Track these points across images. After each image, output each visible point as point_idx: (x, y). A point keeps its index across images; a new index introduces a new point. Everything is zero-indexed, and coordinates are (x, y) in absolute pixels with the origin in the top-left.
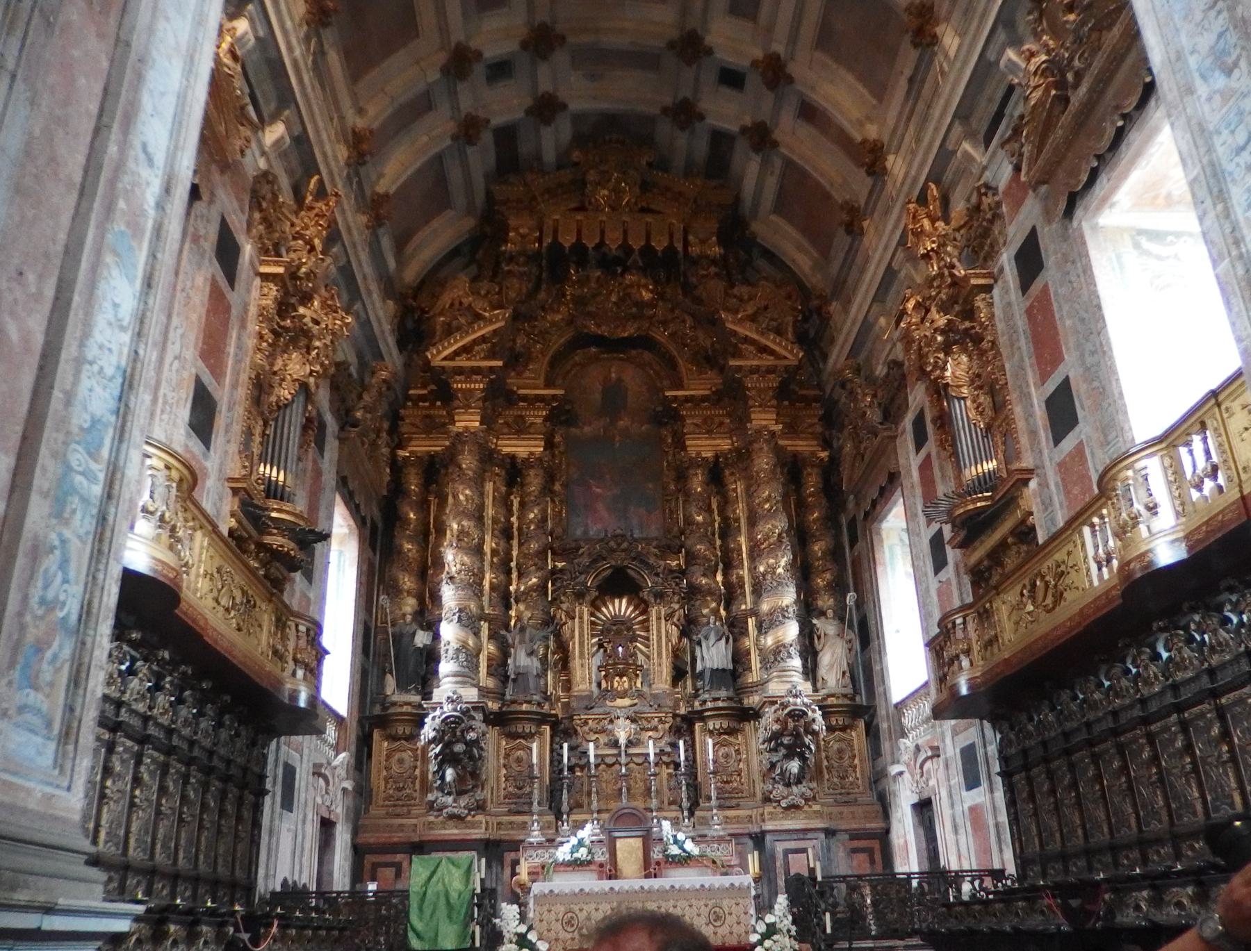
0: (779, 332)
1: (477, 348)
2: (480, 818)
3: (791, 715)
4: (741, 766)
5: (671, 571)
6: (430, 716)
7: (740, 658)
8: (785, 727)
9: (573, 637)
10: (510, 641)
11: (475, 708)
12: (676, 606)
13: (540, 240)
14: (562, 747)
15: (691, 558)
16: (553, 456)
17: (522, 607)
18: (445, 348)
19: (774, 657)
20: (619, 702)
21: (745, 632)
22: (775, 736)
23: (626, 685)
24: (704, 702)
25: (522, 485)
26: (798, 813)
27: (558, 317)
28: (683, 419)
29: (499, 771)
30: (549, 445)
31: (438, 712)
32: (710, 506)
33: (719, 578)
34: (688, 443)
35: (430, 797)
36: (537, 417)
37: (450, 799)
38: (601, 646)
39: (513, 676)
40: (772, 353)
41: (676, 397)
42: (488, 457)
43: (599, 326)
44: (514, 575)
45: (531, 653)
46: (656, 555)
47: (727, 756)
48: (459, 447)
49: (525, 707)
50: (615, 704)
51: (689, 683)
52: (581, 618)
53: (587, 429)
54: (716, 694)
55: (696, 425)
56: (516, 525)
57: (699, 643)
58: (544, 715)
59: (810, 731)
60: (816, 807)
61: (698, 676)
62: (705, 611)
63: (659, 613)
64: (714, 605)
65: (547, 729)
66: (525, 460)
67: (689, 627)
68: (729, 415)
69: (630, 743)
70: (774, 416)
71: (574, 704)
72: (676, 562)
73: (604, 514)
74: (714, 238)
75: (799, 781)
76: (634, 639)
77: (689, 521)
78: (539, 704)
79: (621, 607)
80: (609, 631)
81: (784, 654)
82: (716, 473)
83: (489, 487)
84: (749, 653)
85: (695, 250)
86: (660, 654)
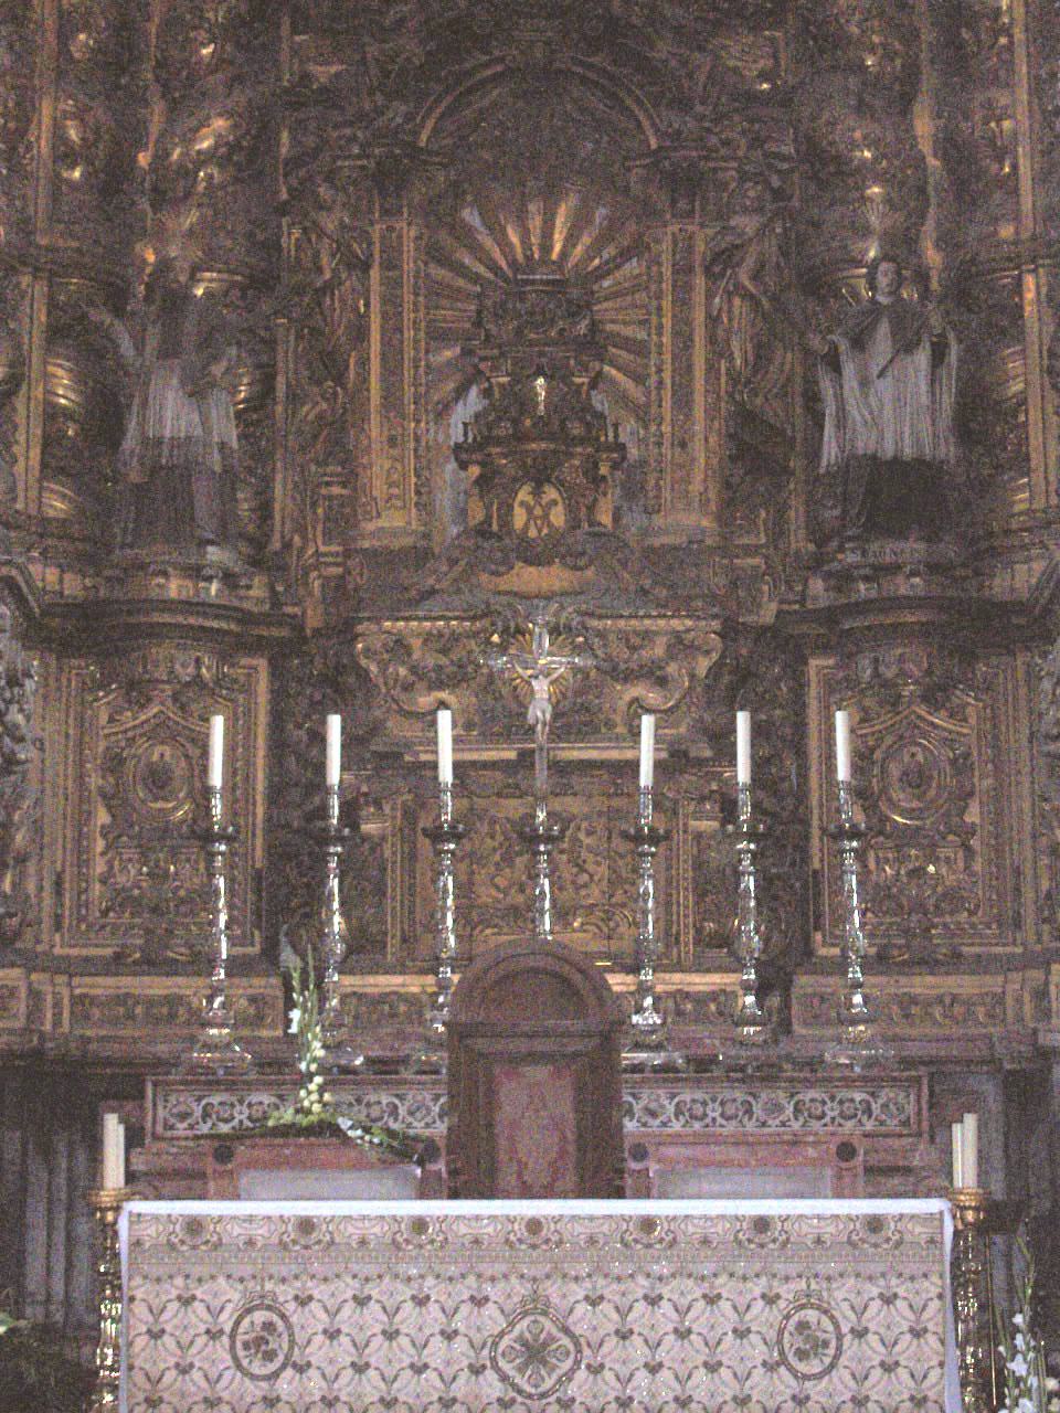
4: (973, 815)
9: (360, 334)
10: (126, 346)
12: (748, 224)
14: (319, 739)
20: (528, 577)
23: (558, 517)
24: (843, 580)
29: (85, 817)
39: (135, 477)
46: (678, 30)
49: (175, 588)
50: (505, 583)
51: (796, 514)
52: (390, 265)
54: (886, 550)
58: (246, 618)
65: (262, 663)
78: (229, 579)
86: (683, 402)
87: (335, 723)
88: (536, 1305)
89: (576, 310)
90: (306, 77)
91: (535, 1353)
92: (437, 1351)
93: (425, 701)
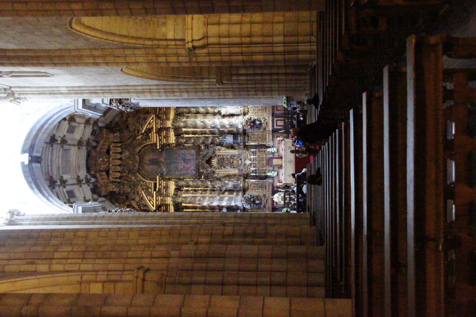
0: (145, 119)
1: (149, 199)
2: (267, 196)
3: (246, 123)
4: (256, 134)
5: (205, 148)
6: (245, 206)
7: (230, 133)
8: (249, 125)
9: (224, 174)
11: (243, 196)
13: (115, 182)
15: (203, 143)
16: (172, 179)
17: (216, 186)
18: (150, 207)
19: (231, 126)
20: (240, 162)
21: (223, 131)
22: (251, 128)
25: (182, 187)
26: (268, 122)
27: (133, 177)
28: (164, 144)
30: (169, 179)
31: (244, 205)
32: (189, 137)
33: (207, 136)
34: (171, 143)
35: (262, 206)
36: (164, 183)
37: (263, 202)
38: (224, 167)
40: (150, 121)
41: (159, 146)
42: (176, 195)
43: (136, 167)
44: (206, 189)
45: (228, 184)
47: (254, 138)
48: (176, 202)
49: (241, 185)
51: (234, 145)
52: (219, 172)
53: (164, 169)
55: (166, 140)
56: (192, 189)
57: (226, 143)
59: (250, 119)
60: (267, 118)
61: (234, 143)
62: (218, 141)
63: (218, 152)
64: (217, 139)
65: (247, 180)
66: (176, 186)
67: (221, 144)
68: (163, 131)
69: (250, 160)
70: (168, 121)
71: (240, 174)
72: (203, 147)
73: (189, 165)
74: (115, 134)
75: (261, 122)
76: (223, 159)
77: (193, 143)
78: (241, 182)
79: (214, 162)
80: (221, 165)
81: (232, 124)
82: (178, 135)
83: (184, 195)
84: (229, 130)
85: (118, 140)
86: (228, 152)
87: (251, 174)
88: (288, 162)
89: (221, 160)
90: (204, 178)
91: (291, 162)
92: (291, 167)
93: (249, 170)
